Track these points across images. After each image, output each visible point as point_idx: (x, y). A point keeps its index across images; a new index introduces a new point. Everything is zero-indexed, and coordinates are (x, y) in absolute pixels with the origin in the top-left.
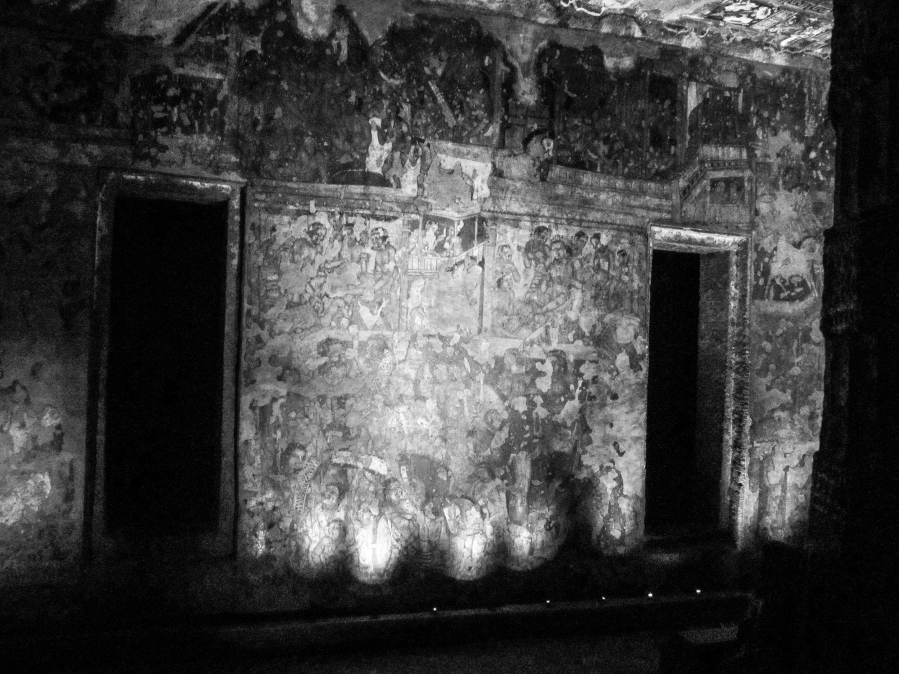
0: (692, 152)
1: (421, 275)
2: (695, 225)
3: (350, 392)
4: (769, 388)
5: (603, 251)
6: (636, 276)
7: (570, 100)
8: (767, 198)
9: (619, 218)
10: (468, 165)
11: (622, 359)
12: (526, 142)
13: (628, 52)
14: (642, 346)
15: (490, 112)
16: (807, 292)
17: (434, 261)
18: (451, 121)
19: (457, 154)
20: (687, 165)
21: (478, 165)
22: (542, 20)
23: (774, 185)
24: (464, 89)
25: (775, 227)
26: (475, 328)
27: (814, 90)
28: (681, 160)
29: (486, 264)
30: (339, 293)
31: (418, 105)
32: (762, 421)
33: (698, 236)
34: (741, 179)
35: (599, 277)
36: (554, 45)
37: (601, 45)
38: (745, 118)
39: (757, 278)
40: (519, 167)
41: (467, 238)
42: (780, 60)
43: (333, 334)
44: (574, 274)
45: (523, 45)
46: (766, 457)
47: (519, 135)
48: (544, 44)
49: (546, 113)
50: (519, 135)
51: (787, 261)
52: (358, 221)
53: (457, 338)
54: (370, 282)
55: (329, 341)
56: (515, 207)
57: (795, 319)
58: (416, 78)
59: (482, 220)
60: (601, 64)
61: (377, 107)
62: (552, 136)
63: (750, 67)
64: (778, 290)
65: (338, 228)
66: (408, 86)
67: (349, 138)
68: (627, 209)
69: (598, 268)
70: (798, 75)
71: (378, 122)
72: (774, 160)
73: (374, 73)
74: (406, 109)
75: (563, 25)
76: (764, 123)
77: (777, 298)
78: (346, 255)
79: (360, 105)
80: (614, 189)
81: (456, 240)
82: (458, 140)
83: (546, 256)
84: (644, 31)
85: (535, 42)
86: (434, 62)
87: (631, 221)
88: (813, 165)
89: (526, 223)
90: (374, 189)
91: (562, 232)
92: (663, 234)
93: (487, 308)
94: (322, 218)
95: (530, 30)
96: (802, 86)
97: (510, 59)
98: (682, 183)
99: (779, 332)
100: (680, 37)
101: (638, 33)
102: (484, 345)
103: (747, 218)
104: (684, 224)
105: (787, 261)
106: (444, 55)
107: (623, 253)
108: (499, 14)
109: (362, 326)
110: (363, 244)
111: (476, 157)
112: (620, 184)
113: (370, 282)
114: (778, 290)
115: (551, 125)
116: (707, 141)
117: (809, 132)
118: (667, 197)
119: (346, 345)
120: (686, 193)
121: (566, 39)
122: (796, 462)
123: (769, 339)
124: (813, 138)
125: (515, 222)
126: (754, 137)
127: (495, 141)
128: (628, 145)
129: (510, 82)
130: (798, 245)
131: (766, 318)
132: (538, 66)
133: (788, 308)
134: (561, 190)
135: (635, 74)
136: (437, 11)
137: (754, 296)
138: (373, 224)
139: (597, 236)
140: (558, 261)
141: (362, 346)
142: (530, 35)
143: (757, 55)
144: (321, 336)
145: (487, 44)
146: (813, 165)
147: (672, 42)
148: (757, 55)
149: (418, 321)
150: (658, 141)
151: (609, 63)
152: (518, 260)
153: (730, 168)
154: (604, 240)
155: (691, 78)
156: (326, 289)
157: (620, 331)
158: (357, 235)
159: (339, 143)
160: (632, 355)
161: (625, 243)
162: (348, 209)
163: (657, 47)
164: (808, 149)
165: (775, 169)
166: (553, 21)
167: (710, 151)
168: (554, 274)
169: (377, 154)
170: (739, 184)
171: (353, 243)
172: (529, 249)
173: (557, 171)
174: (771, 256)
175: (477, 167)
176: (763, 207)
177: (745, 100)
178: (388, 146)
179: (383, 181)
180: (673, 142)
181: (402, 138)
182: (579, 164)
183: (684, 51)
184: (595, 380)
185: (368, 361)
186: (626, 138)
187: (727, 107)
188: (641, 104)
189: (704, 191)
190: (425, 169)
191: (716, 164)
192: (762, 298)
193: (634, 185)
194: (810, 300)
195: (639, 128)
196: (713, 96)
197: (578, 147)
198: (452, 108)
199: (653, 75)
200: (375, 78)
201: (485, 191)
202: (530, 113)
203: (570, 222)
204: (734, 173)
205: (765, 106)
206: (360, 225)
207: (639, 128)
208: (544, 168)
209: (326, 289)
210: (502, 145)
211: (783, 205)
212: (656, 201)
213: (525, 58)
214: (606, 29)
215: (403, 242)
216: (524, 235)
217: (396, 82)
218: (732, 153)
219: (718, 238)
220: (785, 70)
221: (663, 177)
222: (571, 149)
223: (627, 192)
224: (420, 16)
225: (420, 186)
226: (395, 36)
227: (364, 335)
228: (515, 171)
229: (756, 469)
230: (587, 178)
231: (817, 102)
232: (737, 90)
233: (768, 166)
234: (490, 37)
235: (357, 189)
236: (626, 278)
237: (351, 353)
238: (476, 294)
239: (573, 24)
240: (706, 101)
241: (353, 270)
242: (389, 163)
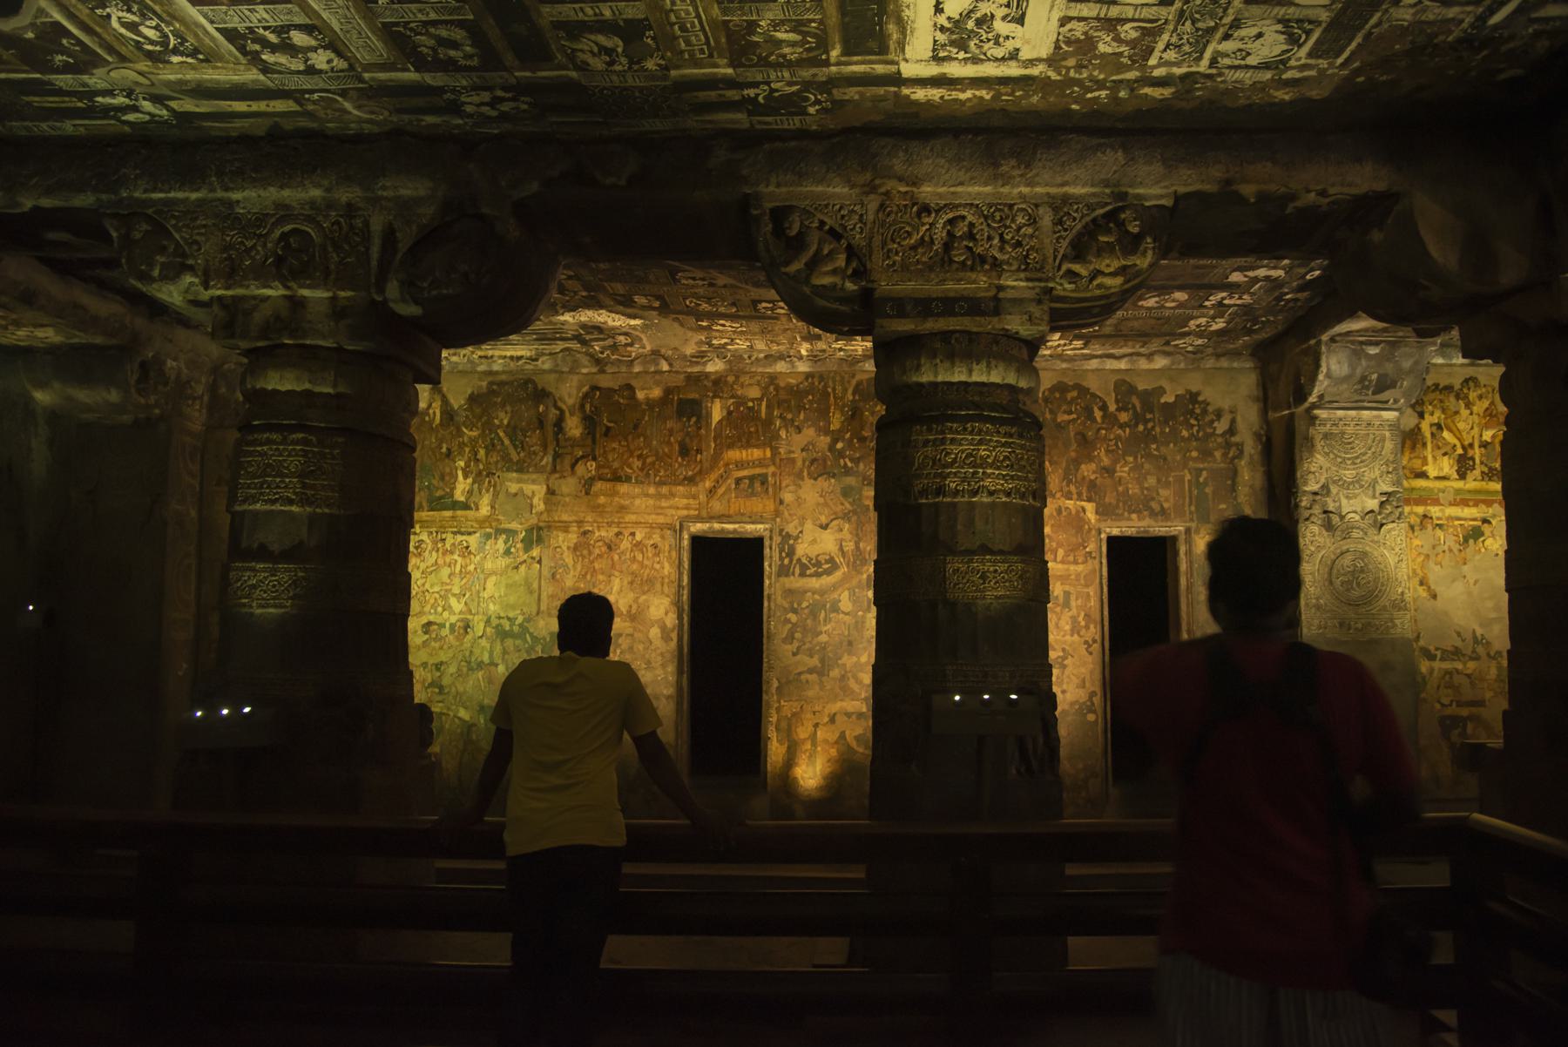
0: (716, 458)
1: (494, 573)
2: (721, 518)
3: (444, 659)
4: (794, 654)
5: (638, 545)
6: (667, 565)
7: (608, 429)
8: (792, 488)
9: (651, 518)
10: (528, 488)
11: (655, 632)
12: (573, 466)
13: (657, 383)
14: (671, 620)
15: (545, 447)
16: (835, 567)
17: (502, 562)
18: (514, 456)
19: (519, 481)
20: (712, 468)
21: (534, 487)
22: (584, 371)
23: (800, 476)
24: (524, 432)
25: (800, 513)
26: (534, 611)
27: (839, 388)
28: (706, 465)
29: (544, 562)
30: (436, 589)
31: (491, 448)
32: (789, 682)
33: (730, 527)
34: (765, 476)
35: (635, 567)
36: (594, 388)
37: (634, 383)
38: (769, 422)
39: (781, 559)
40: (568, 486)
41: (528, 544)
42: (803, 367)
43: (432, 618)
44: (613, 566)
45: (569, 392)
46: (794, 715)
47: (568, 461)
48: (585, 389)
49: (589, 441)
50: (568, 461)
51: (814, 541)
52: (449, 537)
53: (520, 619)
54: (456, 580)
55: (430, 623)
56: (565, 517)
57: (822, 592)
58: (489, 427)
59: (540, 529)
60: (633, 397)
61: (461, 453)
62: (594, 459)
63: (773, 378)
64: (804, 568)
65: (435, 543)
66: (483, 435)
67: (442, 478)
68: (658, 510)
69: (634, 559)
70: (821, 378)
71: (462, 464)
72: (798, 455)
73: (459, 429)
74: (482, 452)
75: (602, 371)
76: (787, 424)
77: (802, 575)
78: (440, 561)
79: (449, 454)
80: (647, 495)
81: (519, 545)
82: (520, 471)
83: (590, 553)
84: (670, 365)
85: (579, 388)
86: (502, 415)
87: (661, 519)
88: (841, 454)
89: (574, 528)
90: (459, 513)
91: (603, 533)
92: (698, 528)
93: (544, 596)
94: (424, 536)
95: (575, 379)
96: (826, 386)
97: (560, 404)
98: (708, 484)
99: (804, 605)
100: (705, 364)
101: (665, 367)
102: (541, 623)
103: (772, 507)
104: (711, 518)
105: (814, 541)
106: (508, 408)
107: (655, 546)
108: (551, 371)
109: (452, 613)
110: (452, 553)
111: (534, 482)
112: (652, 490)
113: (456, 580)
114: (804, 568)
115: (593, 450)
116: (731, 446)
117: (835, 425)
118: (694, 497)
119: (442, 626)
120: (711, 492)
121: (605, 382)
122: (826, 719)
123: (795, 611)
124: (839, 431)
125: (566, 530)
126: (778, 437)
127: (549, 468)
128: (659, 458)
129: (559, 423)
130: (825, 527)
131: (789, 592)
132: (582, 406)
133: (814, 583)
134: (602, 500)
135: (664, 400)
136: (504, 377)
137: (779, 575)
138: (460, 538)
139: (633, 534)
140: (600, 556)
141: (452, 626)
142: (575, 383)
143: (781, 367)
144: (424, 620)
145: (541, 395)
146: (841, 454)
147: (696, 369)
148: (781, 367)
149: (492, 607)
150: (684, 451)
151: (640, 395)
152: (569, 559)
153: (754, 466)
154: (638, 537)
155: (715, 396)
156: (427, 586)
157: (652, 609)
158: (448, 546)
159: (435, 482)
160: (663, 628)
161: (656, 538)
162: (442, 529)
163: (682, 377)
164: (835, 441)
165: (799, 463)
166: (594, 370)
167: (734, 454)
168: (596, 565)
169: (462, 487)
170: (763, 480)
171: (445, 552)
172: (575, 548)
173: (599, 485)
174: (797, 538)
175: (536, 490)
176: (788, 497)
177: (768, 407)
178: (470, 480)
179: (466, 506)
180: (699, 451)
181: (479, 473)
182: (617, 478)
183: (707, 375)
184: (631, 648)
185: (457, 639)
186: (657, 454)
187: (752, 414)
188: (669, 424)
189: (729, 489)
190: (496, 495)
191: (741, 465)
192: (787, 575)
193: (665, 490)
194: (838, 575)
195: (669, 443)
196: (737, 408)
197: (616, 465)
198: (515, 447)
199: (680, 400)
200: (460, 433)
201: (542, 507)
202: (574, 443)
203: (610, 524)
204: (758, 471)
205: (789, 409)
206: (450, 539)
207: (669, 443)
208: (588, 484)
209: (427, 586)
210: (554, 470)
211: (811, 492)
212: (685, 501)
213: (570, 402)
214: (637, 369)
215: (481, 549)
216: (573, 537)
217: (475, 433)
218: (756, 453)
219: (749, 527)
220: (808, 376)
221: (691, 480)
222: (609, 467)
223: (659, 496)
224: (491, 383)
225: (493, 507)
226: (473, 399)
227: (453, 619)
228: (565, 490)
229: (784, 724)
230: (623, 488)
231: (842, 398)
232: (761, 399)
233: (793, 461)
234: (543, 390)
235: (448, 514)
236: (657, 566)
237: (445, 632)
238: (535, 585)
239: (609, 369)
240: (730, 413)
241: (445, 572)
242: (470, 492)
